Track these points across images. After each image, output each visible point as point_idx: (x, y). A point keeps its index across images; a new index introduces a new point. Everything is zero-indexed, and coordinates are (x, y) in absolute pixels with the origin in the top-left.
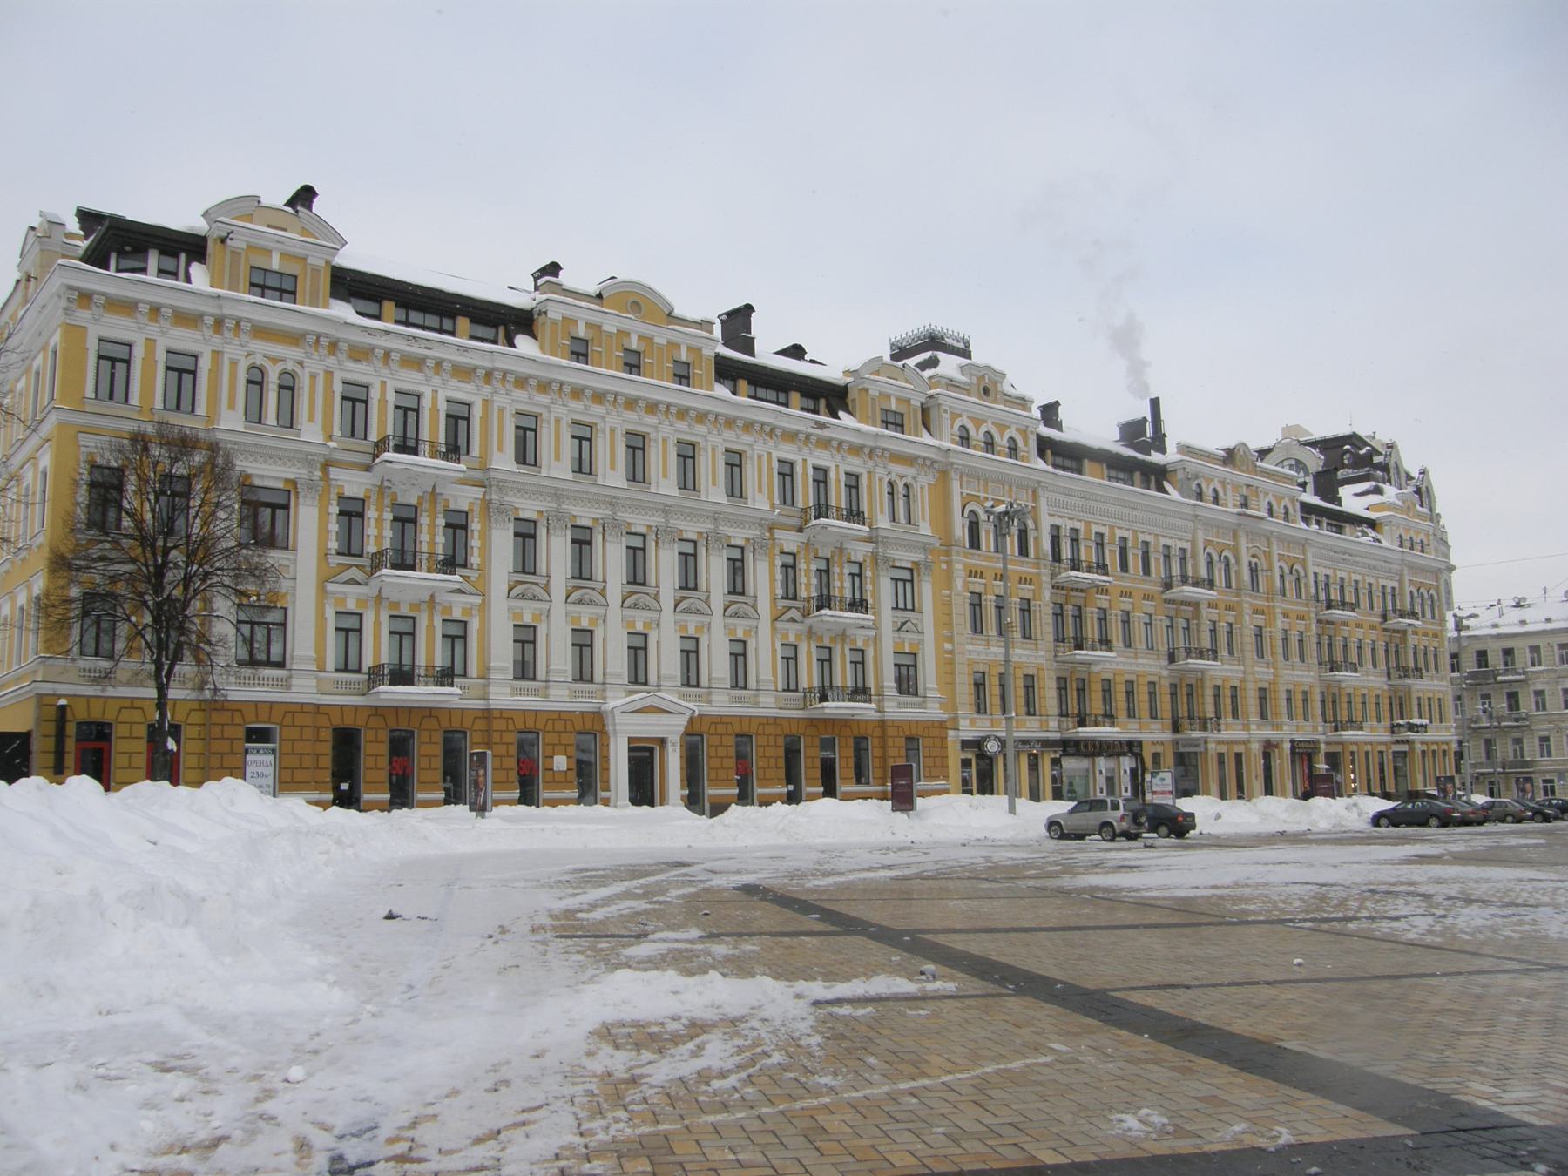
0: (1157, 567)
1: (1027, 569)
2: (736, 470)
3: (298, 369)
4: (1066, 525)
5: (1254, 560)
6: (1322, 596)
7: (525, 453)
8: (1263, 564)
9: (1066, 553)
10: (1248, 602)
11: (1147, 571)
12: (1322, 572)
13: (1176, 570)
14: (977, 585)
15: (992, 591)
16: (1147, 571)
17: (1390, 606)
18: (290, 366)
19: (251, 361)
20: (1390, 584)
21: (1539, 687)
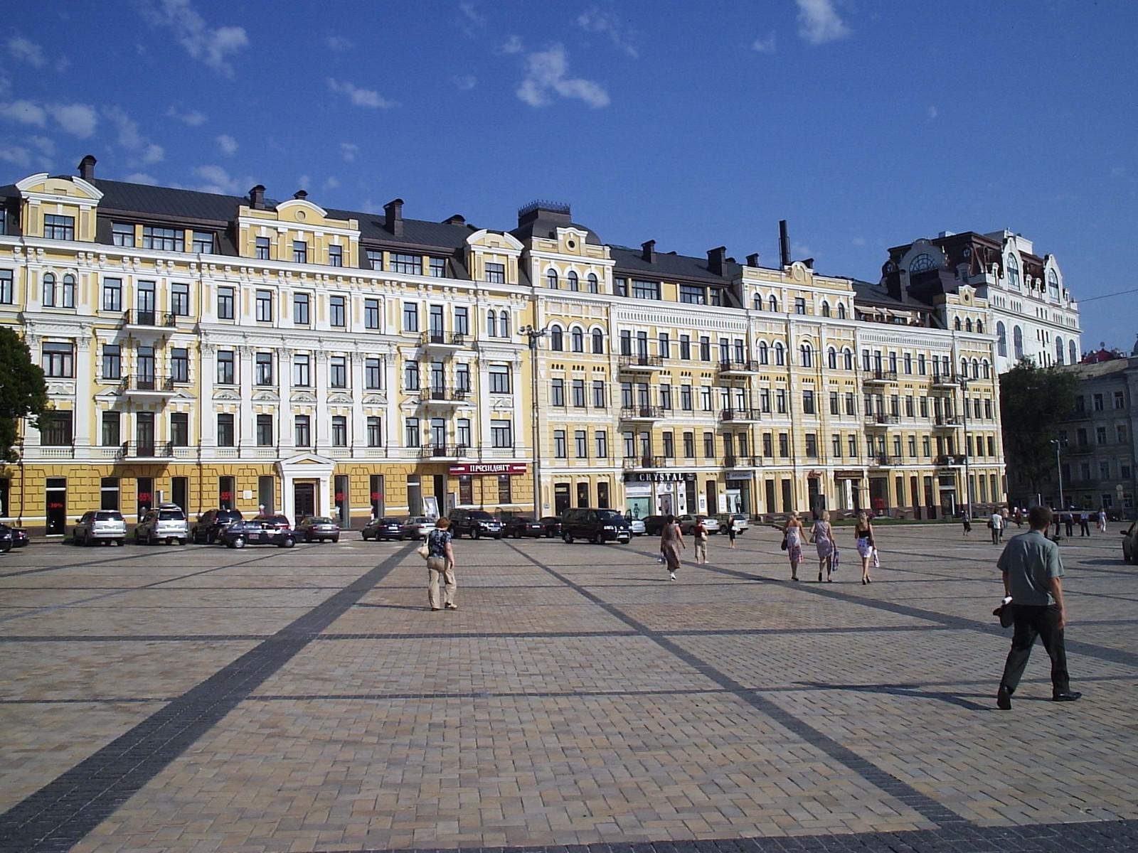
0: (715, 354)
1: (601, 360)
2: (374, 311)
3: (74, 273)
4: (634, 330)
5: (805, 344)
6: (873, 367)
7: (226, 312)
8: (814, 347)
9: (635, 349)
10: (796, 375)
11: (705, 356)
12: (873, 349)
13: (732, 355)
14: (559, 374)
15: (570, 377)
16: (705, 356)
17: (941, 371)
18: (70, 272)
19: (45, 270)
20: (941, 355)
21: (1101, 425)
